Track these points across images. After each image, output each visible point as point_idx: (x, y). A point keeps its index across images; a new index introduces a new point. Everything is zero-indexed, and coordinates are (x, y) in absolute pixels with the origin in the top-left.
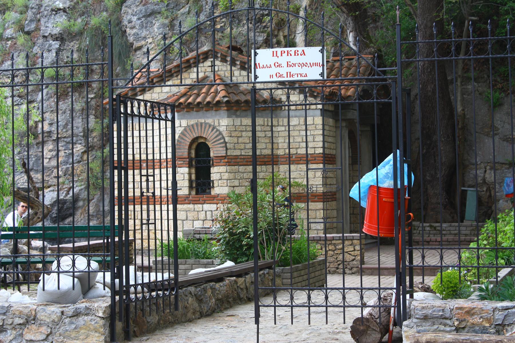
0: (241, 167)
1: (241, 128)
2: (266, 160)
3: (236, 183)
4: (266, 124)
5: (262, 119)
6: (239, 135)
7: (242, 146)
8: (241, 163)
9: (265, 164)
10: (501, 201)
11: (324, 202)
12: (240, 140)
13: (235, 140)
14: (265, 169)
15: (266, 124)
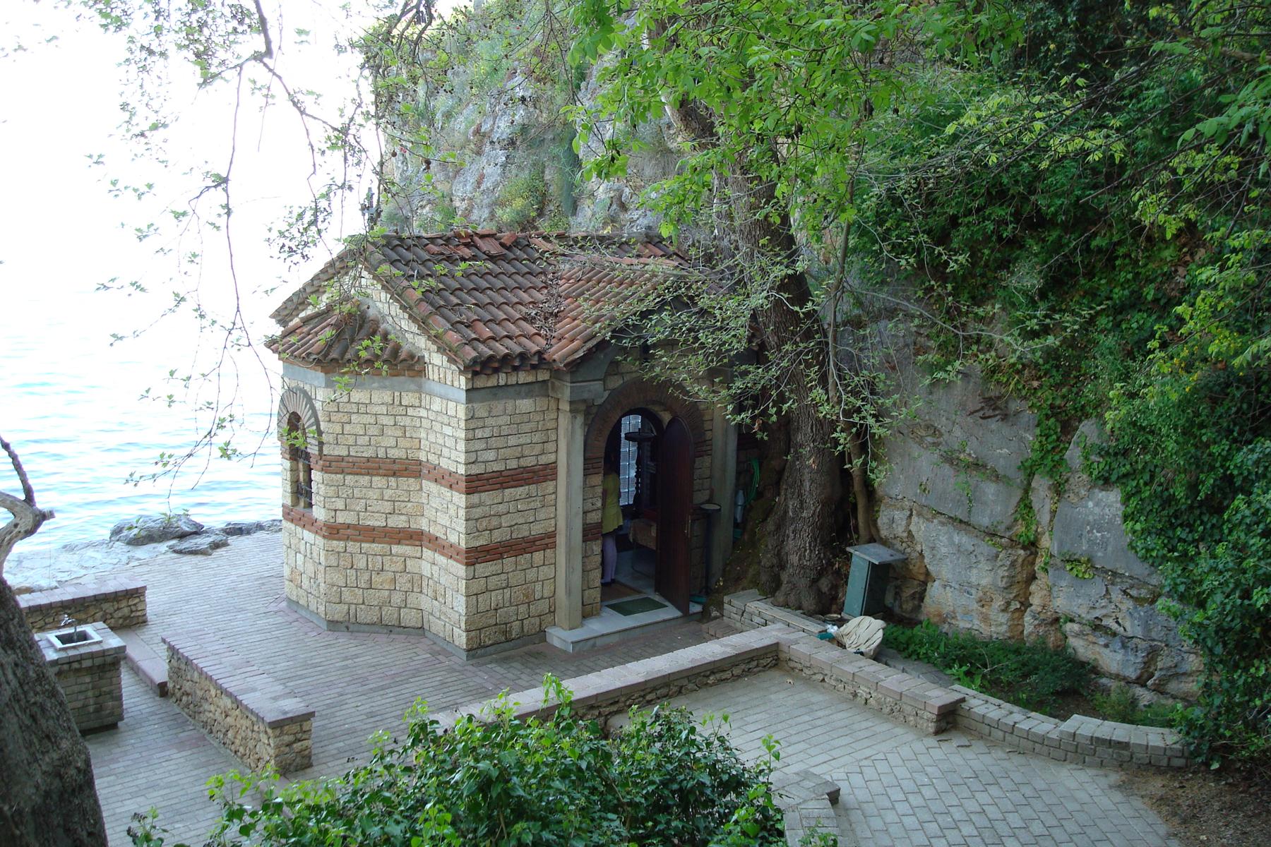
0: (348, 478)
1: (348, 408)
2: (396, 467)
3: (340, 504)
4: (397, 402)
5: (389, 393)
6: (345, 419)
7: (351, 441)
8: (349, 470)
9: (394, 475)
10: (937, 583)
11: (467, 564)
12: (347, 427)
13: (338, 429)
14: (394, 485)
15: (397, 402)
